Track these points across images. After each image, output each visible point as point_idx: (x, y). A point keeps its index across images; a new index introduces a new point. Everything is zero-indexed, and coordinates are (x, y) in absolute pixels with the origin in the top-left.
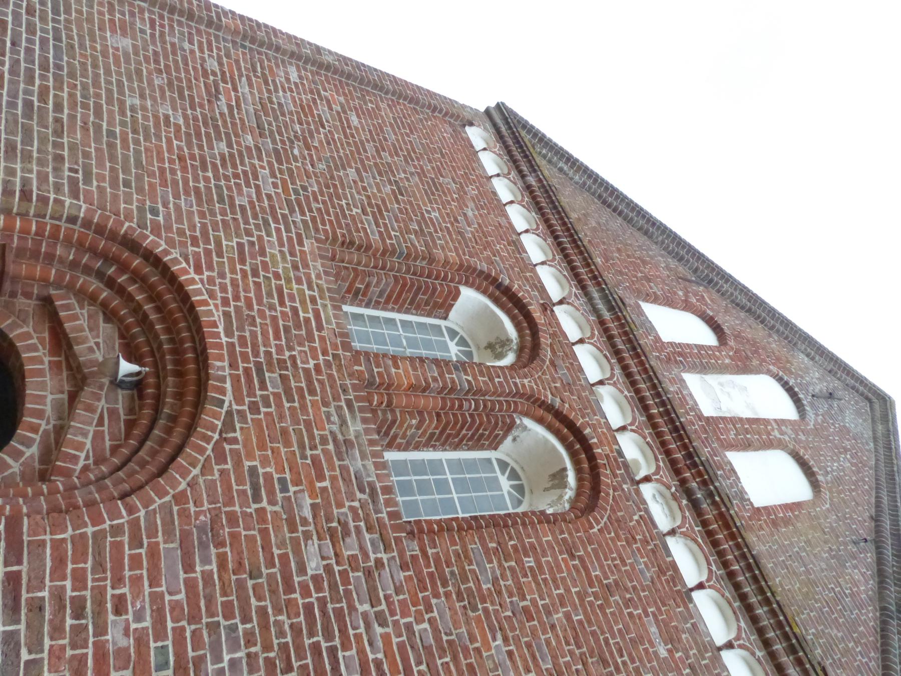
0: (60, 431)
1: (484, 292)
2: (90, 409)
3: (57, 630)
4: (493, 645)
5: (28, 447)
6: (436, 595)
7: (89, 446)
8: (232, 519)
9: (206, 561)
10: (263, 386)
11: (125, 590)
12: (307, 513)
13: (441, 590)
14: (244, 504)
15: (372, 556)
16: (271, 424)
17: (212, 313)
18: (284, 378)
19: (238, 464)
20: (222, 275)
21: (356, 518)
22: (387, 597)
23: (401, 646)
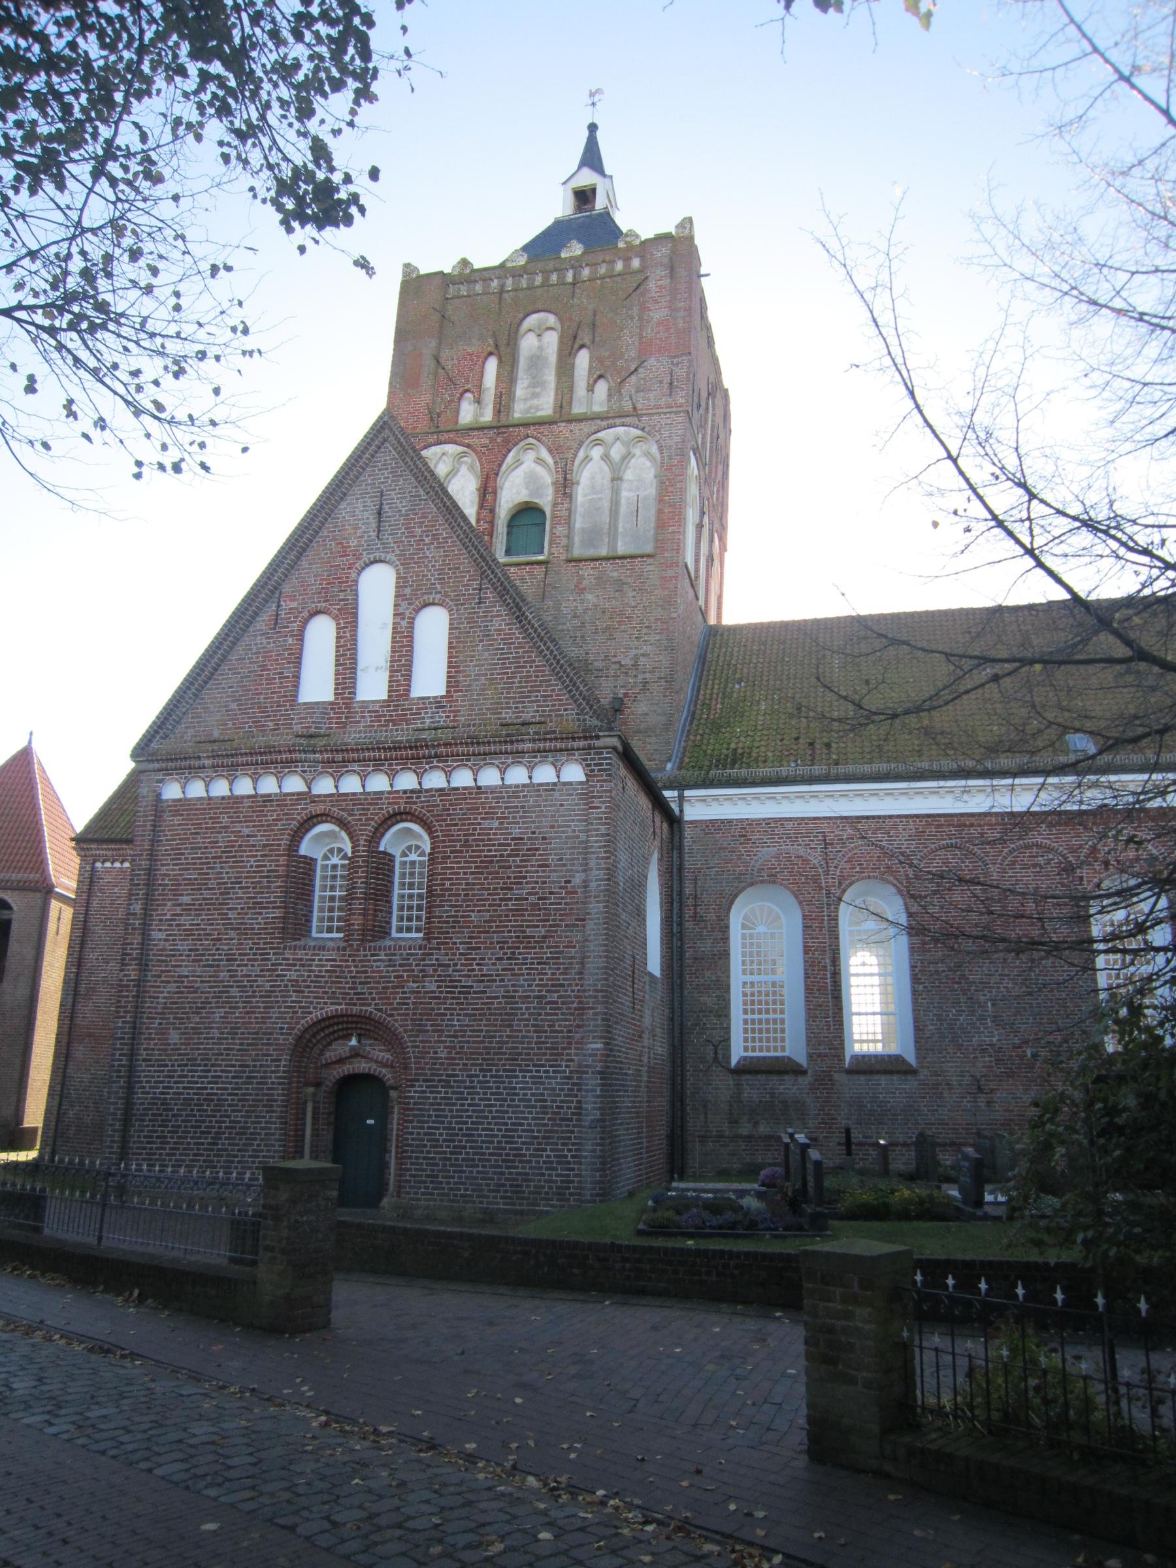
0: (376, 1062)
1: (302, 838)
10: (363, 993)
12: (416, 985)
17: (331, 1009)
18: (360, 983)
19: (395, 1009)
20: (312, 1003)
23: (466, 959)
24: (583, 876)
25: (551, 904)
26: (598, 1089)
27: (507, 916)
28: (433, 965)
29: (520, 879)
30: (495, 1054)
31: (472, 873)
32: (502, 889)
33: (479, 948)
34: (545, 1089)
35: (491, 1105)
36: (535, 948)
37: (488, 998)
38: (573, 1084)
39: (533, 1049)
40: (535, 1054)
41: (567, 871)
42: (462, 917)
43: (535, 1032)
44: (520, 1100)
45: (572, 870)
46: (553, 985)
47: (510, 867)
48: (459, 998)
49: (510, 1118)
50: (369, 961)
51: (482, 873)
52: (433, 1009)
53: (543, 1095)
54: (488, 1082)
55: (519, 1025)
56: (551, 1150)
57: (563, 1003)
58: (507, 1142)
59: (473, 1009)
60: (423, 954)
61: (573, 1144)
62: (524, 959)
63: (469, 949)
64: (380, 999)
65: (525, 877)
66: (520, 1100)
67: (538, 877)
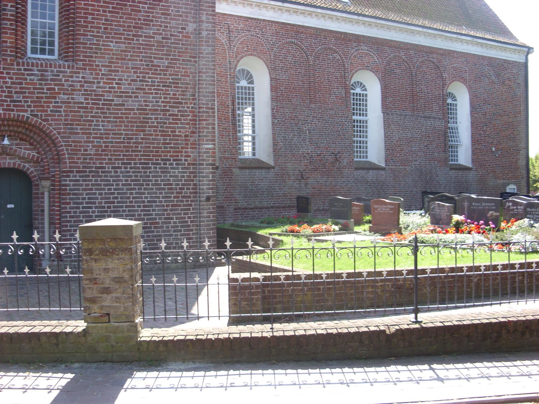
0: (20, 158)
2: (16, 151)
3: (89, 163)
4: (112, 48)
5: (25, 166)
6: (95, 61)
7: (29, 152)
8: (66, 120)
9: (77, 129)
10: (20, 101)
11: (82, 149)
12: (66, 97)
13: (94, 59)
14: (61, 116)
15: (80, 79)
16: (36, 102)
18: (16, 93)
19: (49, 115)
21: (68, 81)
22: (93, 79)
23: (107, 79)
24: (195, 26)
25: (172, 43)
26: (211, 175)
27: (139, 48)
28: (80, 82)
29: (148, 22)
30: (133, 151)
31: (110, 12)
32: (134, 27)
33: (118, 71)
34: (170, 176)
35: (132, 189)
36: (160, 74)
37: (126, 109)
38: (190, 173)
39: (161, 148)
40: (162, 152)
41: (183, 20)
42: (103, 45)
43: (162, 135)
44: (153, 185)
45: (187, 21)
46: (174, 103)
47: (140, 11)
48: (103, 109)
49: (146, 198)
50: (24, 74)
51: (118, 13)
52: (82, 116)
53: (169, 180)
54: (129, 172)
55: (150, 131)
56: (177, 218)
57: (182, 116)
58: (145, 215)
59: (114, 118)
60: (71, 72)
61: (192, 213)
62: (152, 82)
63: (110, 71)
64: (34, 106)
65: (152, 21)
66: (153, 185)
67: (162, 22)
